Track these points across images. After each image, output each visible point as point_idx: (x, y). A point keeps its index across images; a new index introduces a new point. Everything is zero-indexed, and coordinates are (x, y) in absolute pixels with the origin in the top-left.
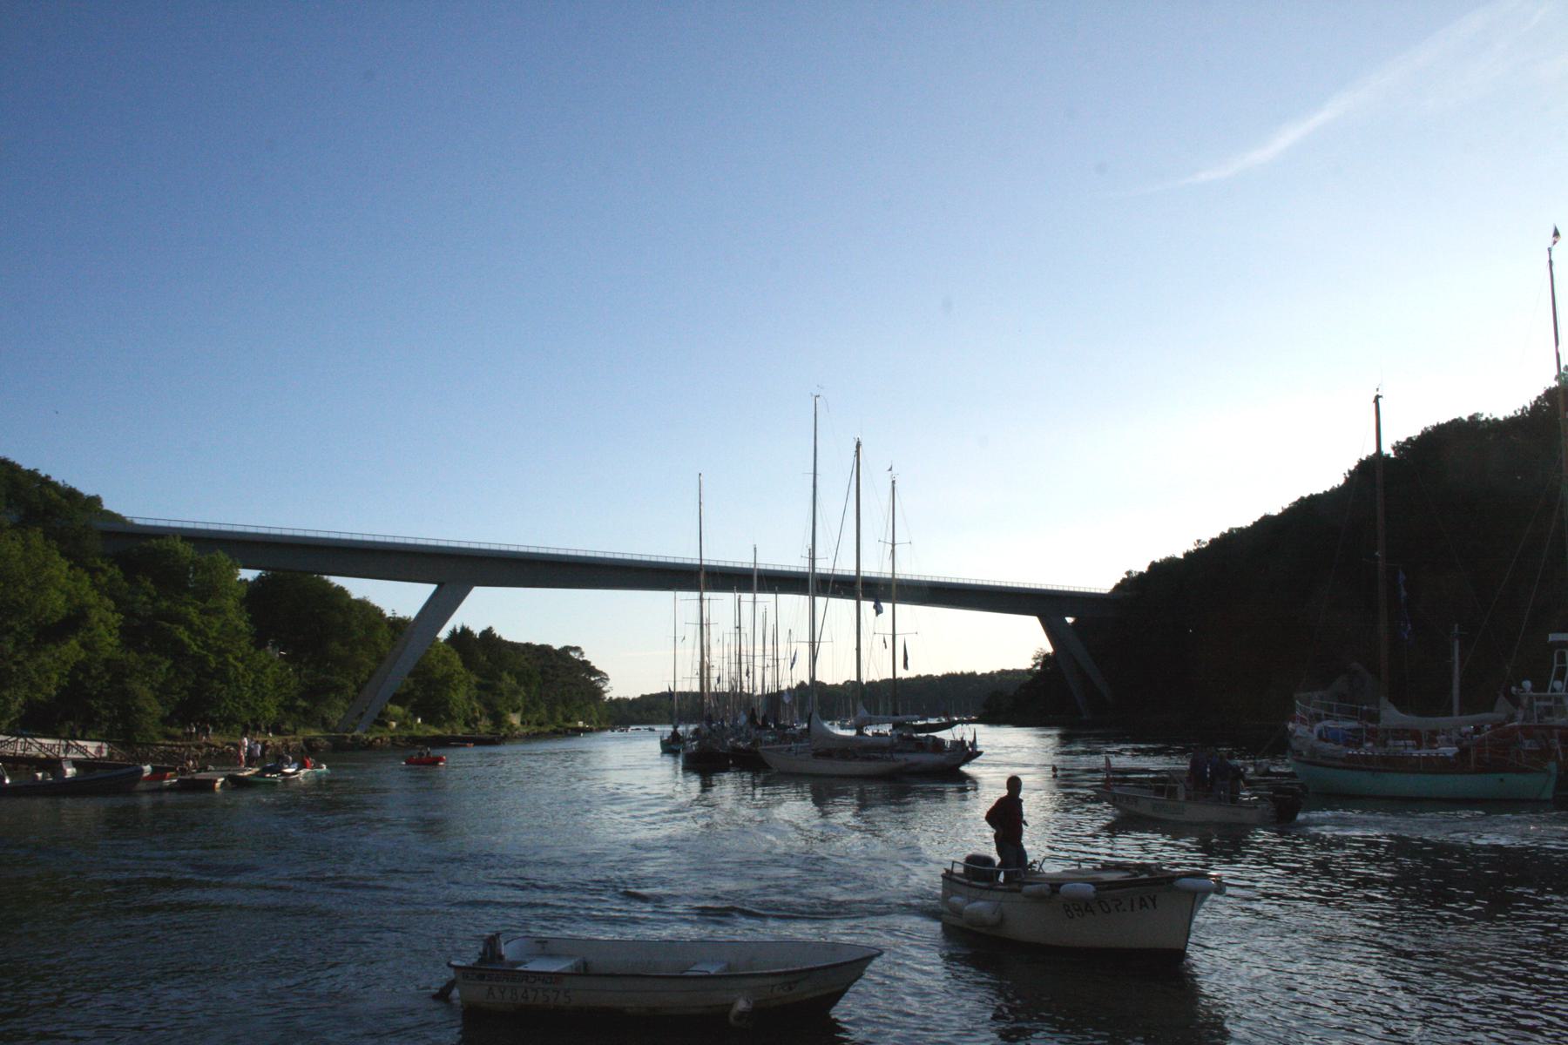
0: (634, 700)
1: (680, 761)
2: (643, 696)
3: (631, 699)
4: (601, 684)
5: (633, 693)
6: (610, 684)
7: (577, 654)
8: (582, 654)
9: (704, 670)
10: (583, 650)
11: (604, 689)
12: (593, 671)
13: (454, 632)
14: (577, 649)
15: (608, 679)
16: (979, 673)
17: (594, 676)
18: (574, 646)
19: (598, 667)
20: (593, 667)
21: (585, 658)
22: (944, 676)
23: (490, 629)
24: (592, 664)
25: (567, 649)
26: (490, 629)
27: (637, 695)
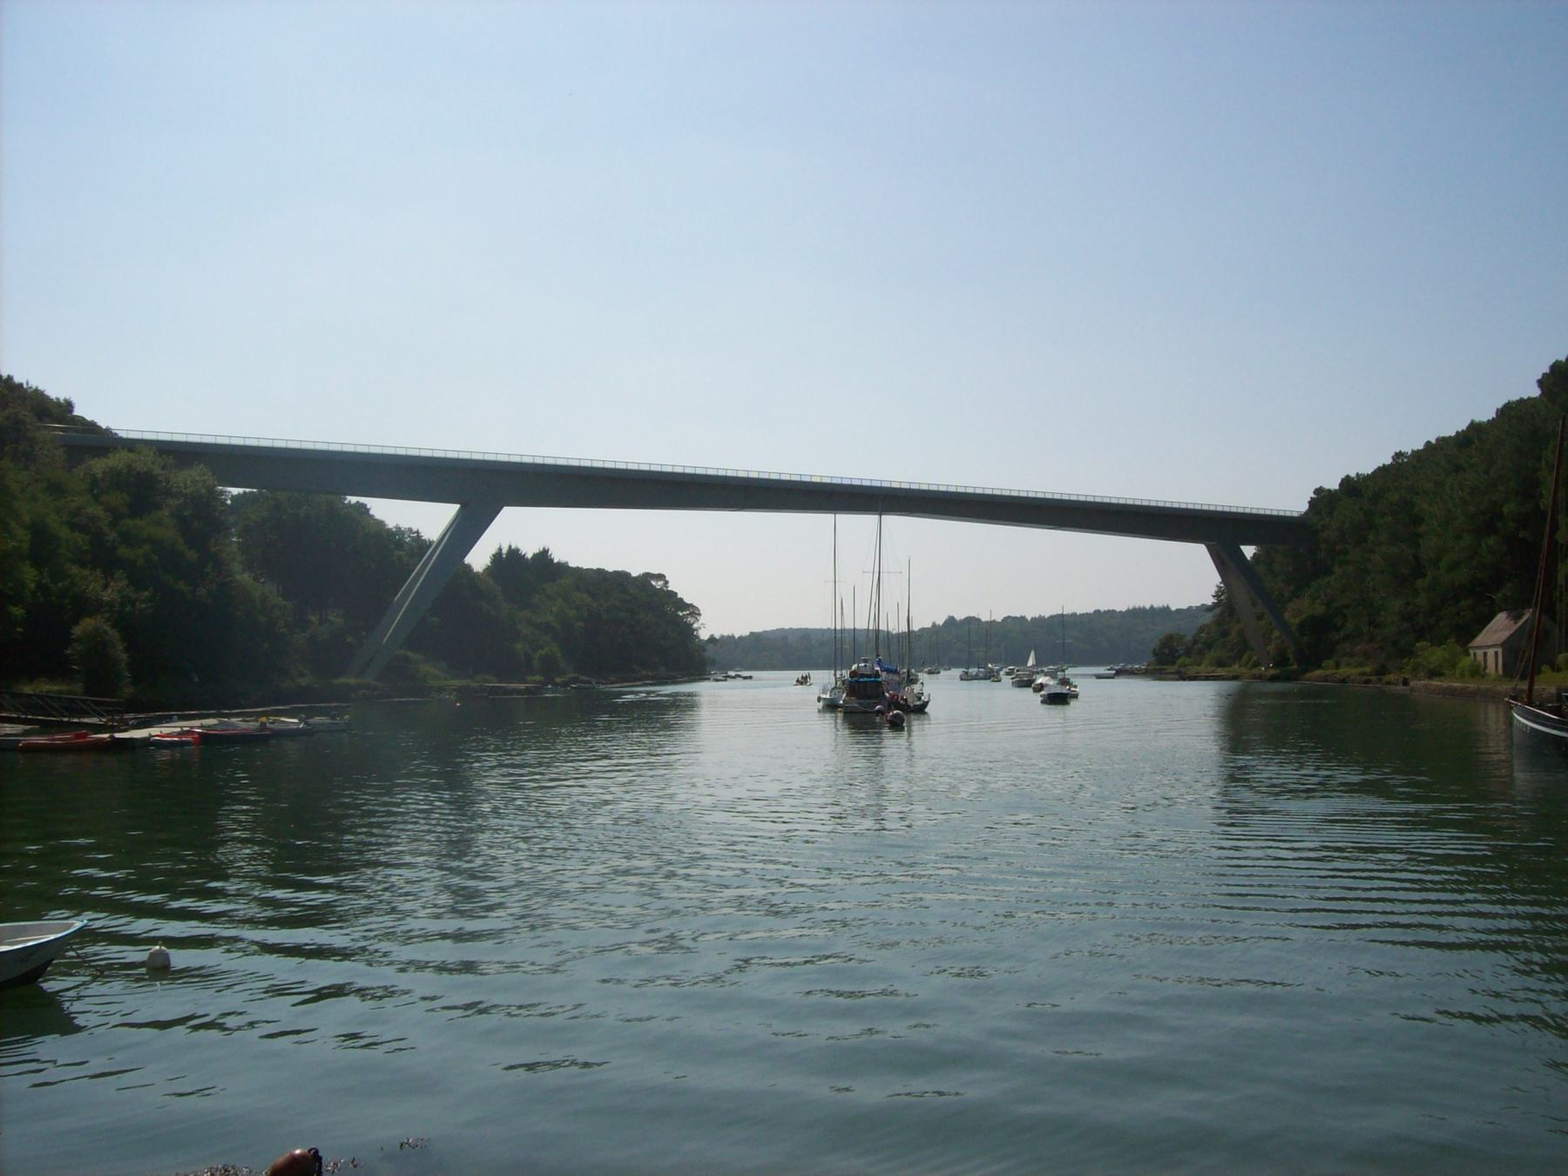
0: (741, 638)
1: (840, 715)
2: (1097, 612)
3: (737, 636)
4: (690, 620)
5: (740, 629)
6: (702, 619)
7: (661, 583)
8: (667, 582)
9: (838, 607)
10: (667, 579)
11: (695, 626)
12: (681, 605)
13: (497, 557)
14: (661, 577)
15: (699, 614)
16: (1173, 608)
17: (682, 611)
18: (656, 573)
19: (688, 600)
20: (681, 600)
21: (669, 589)
22: (1128, 611)
23: (545, 552)
24: (679, 596)
25: (648, 577)
26: (545, 552)
27: (746, 633)
